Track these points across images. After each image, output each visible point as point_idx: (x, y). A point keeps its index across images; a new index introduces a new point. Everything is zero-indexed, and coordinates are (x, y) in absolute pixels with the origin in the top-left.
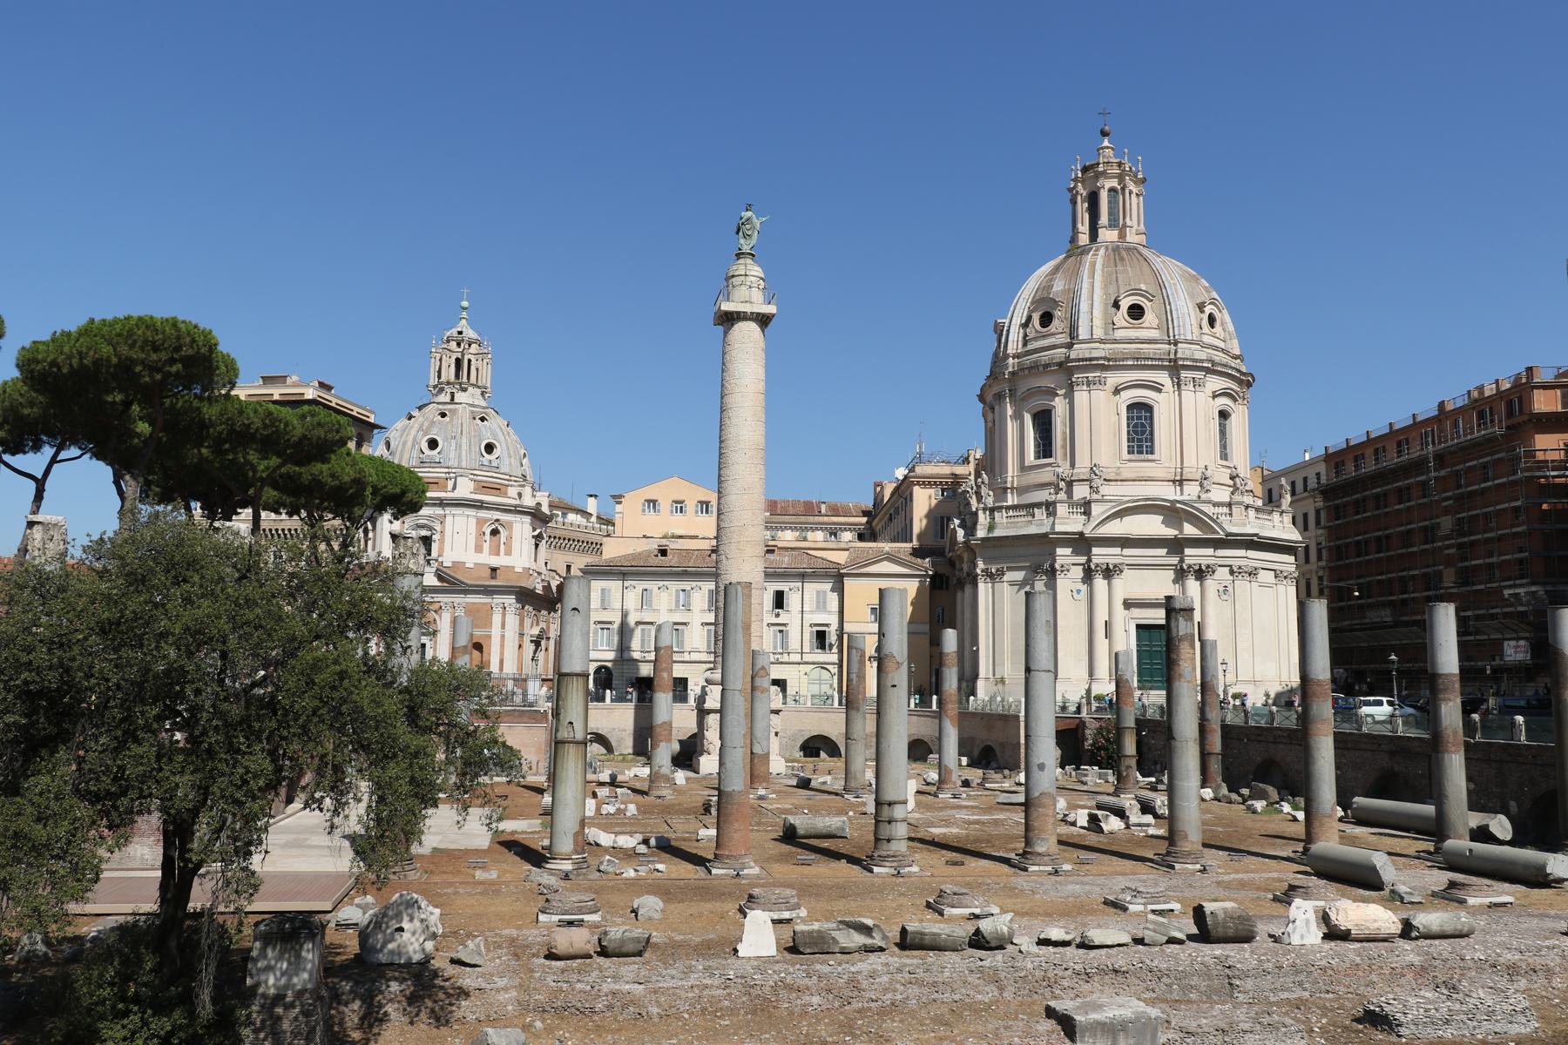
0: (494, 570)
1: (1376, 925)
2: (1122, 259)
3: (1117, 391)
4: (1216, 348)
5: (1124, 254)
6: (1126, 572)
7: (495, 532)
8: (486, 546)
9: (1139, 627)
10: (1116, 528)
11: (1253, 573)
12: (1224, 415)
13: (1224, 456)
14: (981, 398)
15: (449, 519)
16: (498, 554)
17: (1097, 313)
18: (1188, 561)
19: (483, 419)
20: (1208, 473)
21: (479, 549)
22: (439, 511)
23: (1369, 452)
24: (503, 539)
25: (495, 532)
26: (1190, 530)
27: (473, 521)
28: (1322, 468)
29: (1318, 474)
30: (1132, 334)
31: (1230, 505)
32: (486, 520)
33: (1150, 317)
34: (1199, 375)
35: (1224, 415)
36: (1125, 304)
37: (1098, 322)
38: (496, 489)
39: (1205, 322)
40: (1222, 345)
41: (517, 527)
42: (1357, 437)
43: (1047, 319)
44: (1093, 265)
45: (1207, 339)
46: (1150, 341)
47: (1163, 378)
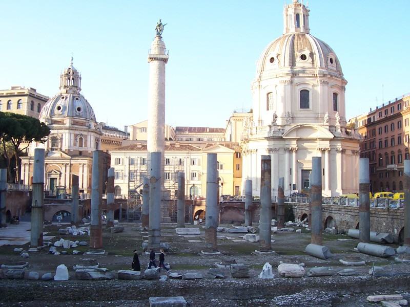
0: (81, 153)
1: (295, 272)
2: (300, 38)
3: (298, 85)
5: (301, 37)
7: (81, 139)
8: (78, 144)
12: (335, 95)
19: (77, 99)
21: (75, 145)
22: (60, 131)
24: (83, 141)
25: (81, 139)
27: (73, 135)
30: (302, 65)
32: (77, 135)
33: (309, 59)
35: (335, 95)
36: (299, 55)
38: (83, 124)
39: (329, 61)
41: (89, 137)
43: (272, 60)
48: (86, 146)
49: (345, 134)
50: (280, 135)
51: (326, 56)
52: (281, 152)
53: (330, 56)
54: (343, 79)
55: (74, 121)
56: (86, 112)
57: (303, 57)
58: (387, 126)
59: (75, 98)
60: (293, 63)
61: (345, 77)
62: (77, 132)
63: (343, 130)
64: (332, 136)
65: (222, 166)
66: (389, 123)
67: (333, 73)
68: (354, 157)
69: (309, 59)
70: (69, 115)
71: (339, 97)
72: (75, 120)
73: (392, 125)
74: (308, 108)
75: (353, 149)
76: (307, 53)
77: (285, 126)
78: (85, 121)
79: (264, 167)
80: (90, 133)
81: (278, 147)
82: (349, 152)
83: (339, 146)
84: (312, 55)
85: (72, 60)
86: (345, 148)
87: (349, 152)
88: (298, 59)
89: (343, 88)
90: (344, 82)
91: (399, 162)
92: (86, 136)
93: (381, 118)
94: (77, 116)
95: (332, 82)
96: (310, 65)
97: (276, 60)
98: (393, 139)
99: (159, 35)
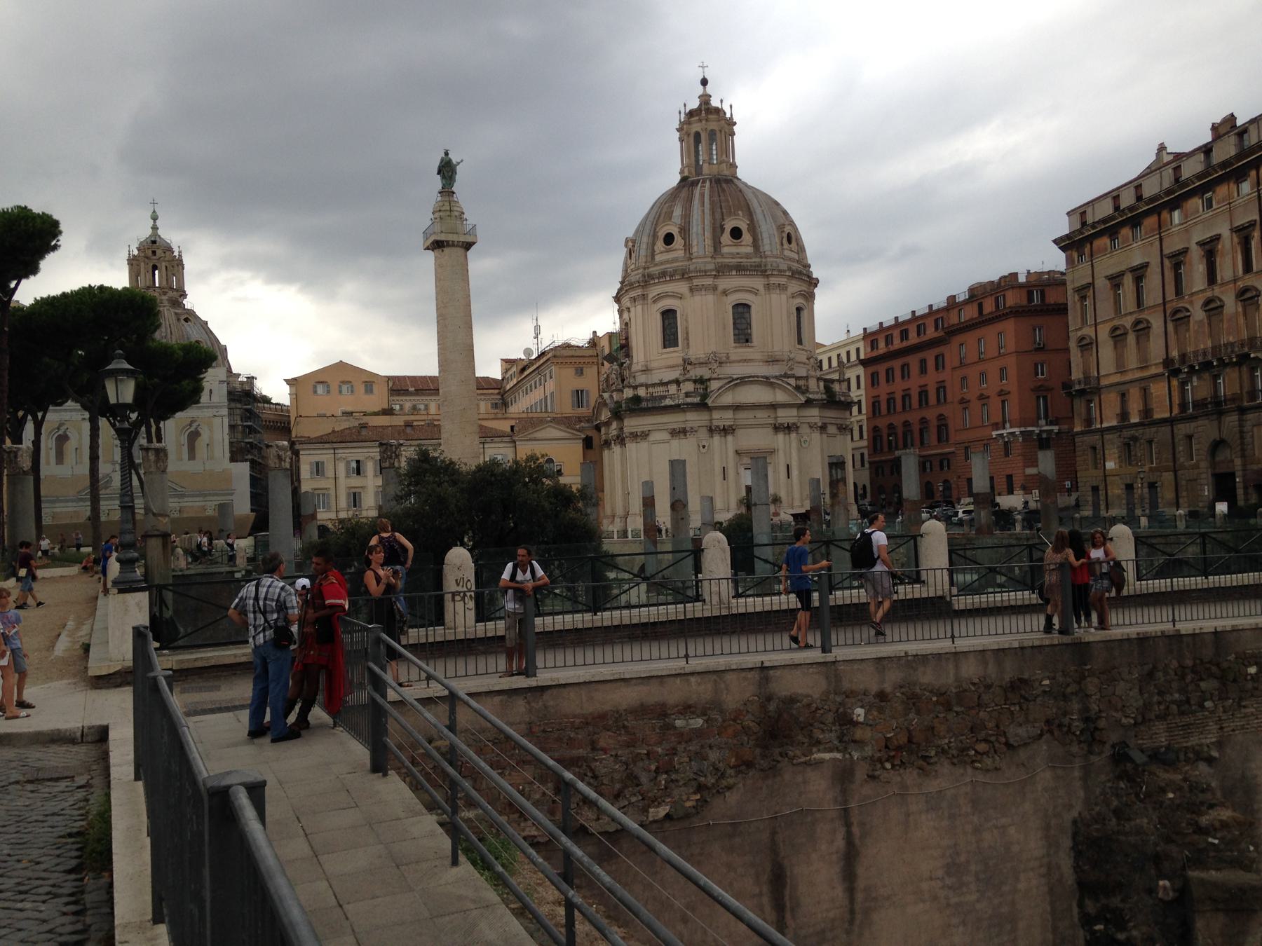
2: (724, 191)
3: (725, 293)
4: (791, 259)
5: (724, 185)
6: (739, 432)
10: (728, 399)
11: (823, 428)
12: (799, 310)
13: (800, 342)
14: (617, 299)
17: (708, 234)
18: (780, 421)
19: (186, 320)
20: (792, 356)
23: (896, 333)
26: (780, 397)
28: (861, 345)
29: (858, 350)
30: (734, 250)
31: (807, 378)
33: (747, 237)
34: (783, 281)
36: (728, 227)
37: (709, 242)
39: (785, 240)
40: (796, 256)
42: (888, 321)
43: (669, 239)
44: (702, 195)
45: (787, 253)
46: (747, 256)
47: (758, 283)
50: (697, 400)
51: (781, 228)
52: (703, 434)
53: (788, 229)
54: (809, 276)
57: (736, 233)
58: (893, 369)
60: (717, 245)
61: (816, 272)
63: (822, 384)
64: (803, 399)
66: (897, 364)
67: (795, 266)
71: (805, 314)
73: (905, 368)
75: (839, 422)
76: (743, 226)
77: (709, 380)
81: (695, 425)
82: (832, 429)
83: (814, 414)
84: (753, 228)
85: (155, 218)
86: (827, 421)
87: (832, 429)
89: (810, 297)
90: (814, 283)
91: (922, 443)
93: (875, 353)
95: (795, 287)
96: (750, 250)
97: (678, 242)
98: (906, 396)
99: (447, 191)
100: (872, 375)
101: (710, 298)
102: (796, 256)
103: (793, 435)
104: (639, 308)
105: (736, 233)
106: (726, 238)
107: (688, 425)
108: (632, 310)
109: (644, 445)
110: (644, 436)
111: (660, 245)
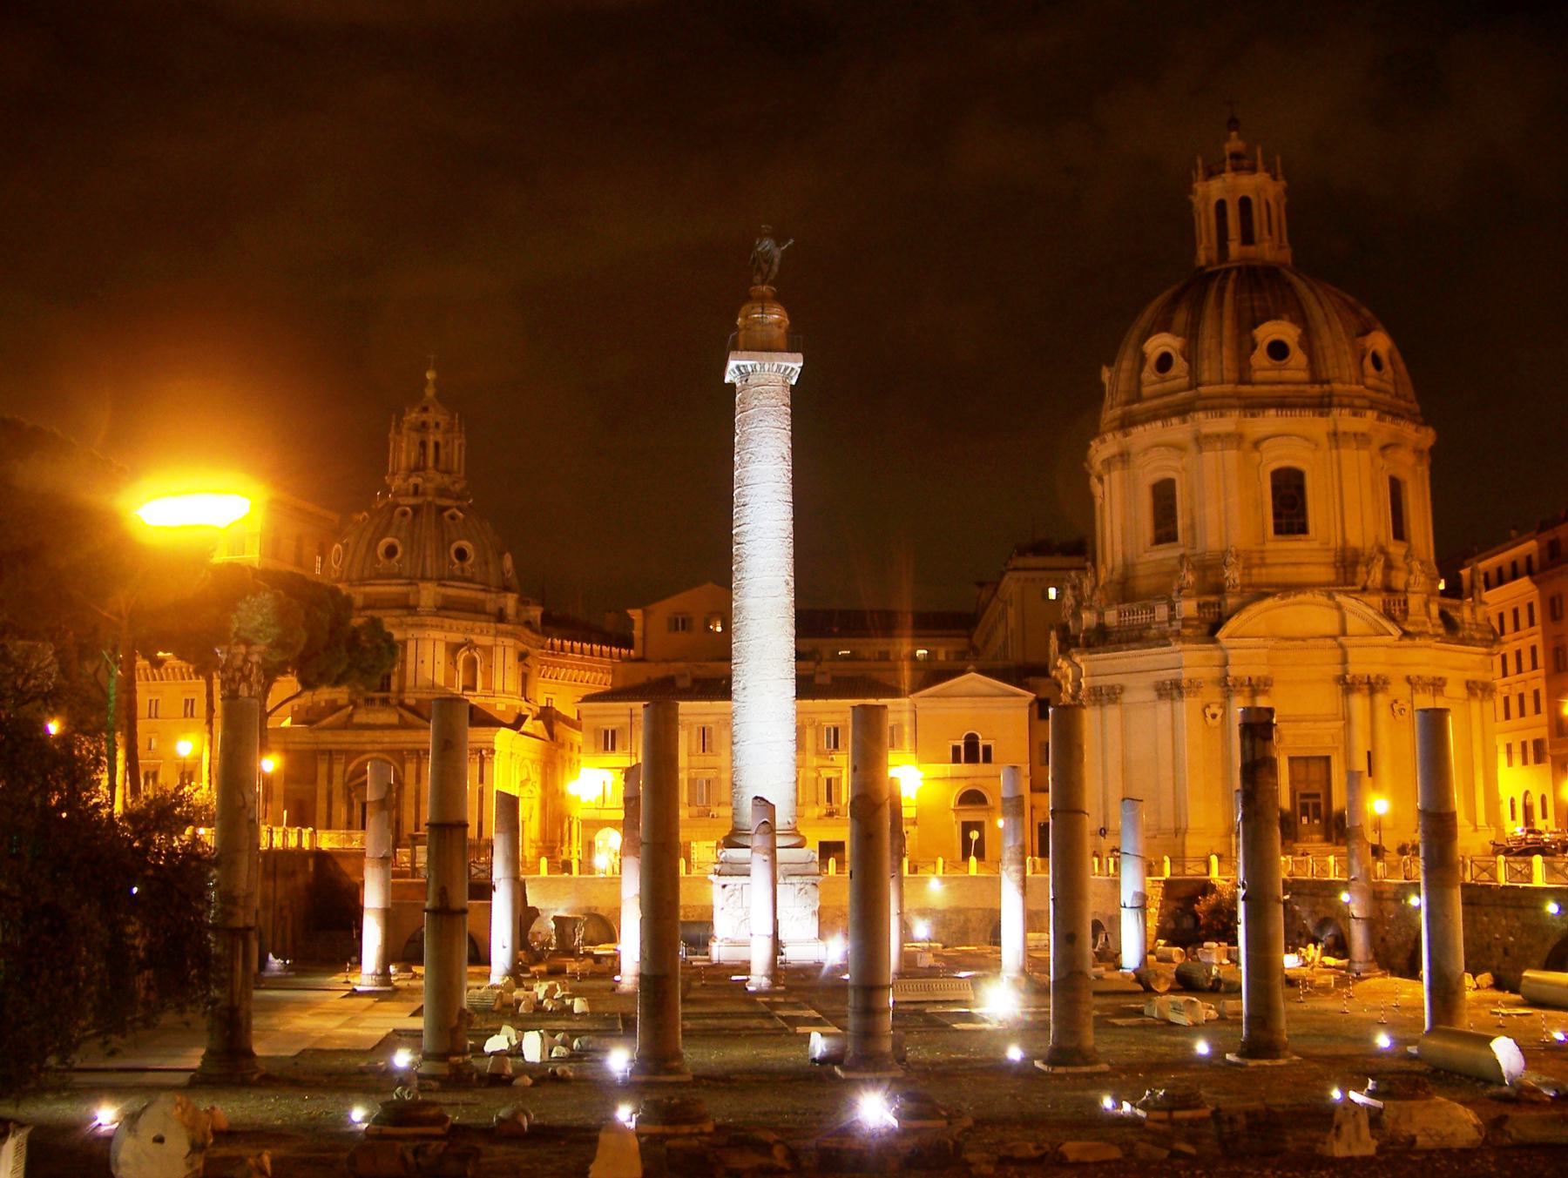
9: (1291, 759)
15: (411, 645)
16: (474, 689)
25: (471, 664)
30: (1273, 375)
32: (458, 647)
39: (1368, 362)
41: (499, 652)
44: (1222, 290)
46: (1299, 383)
48: (488, 686)
49: (1439, 622)
55: (446, 597)
56: (486, 563)
59: (446, 514)
62: (457, 638)
65: (987, 749)
68: (1475, 705)
69: (1297, 357)
70: (428, 574)
72: (450, 592)
74: (1303, 530)
75: (1469, 676)
78: (481, 596)
79: (1253, 749)
80: (500, 640)
88: (1260, 358)
92: (488, 651)
94: (453, 578)
97: (1179, 365)
100: (1552, 600)
101: (1232, 455)
102: (1391, 389)
103: (1380, 698)
104: (1116, 474)
105: (1278, 350)
106: (1260, 358)
107: (1186, 674)
108: (1106, 478)
109: (1113, 712)
110: (1107, 696)
111: (1149, 374)
